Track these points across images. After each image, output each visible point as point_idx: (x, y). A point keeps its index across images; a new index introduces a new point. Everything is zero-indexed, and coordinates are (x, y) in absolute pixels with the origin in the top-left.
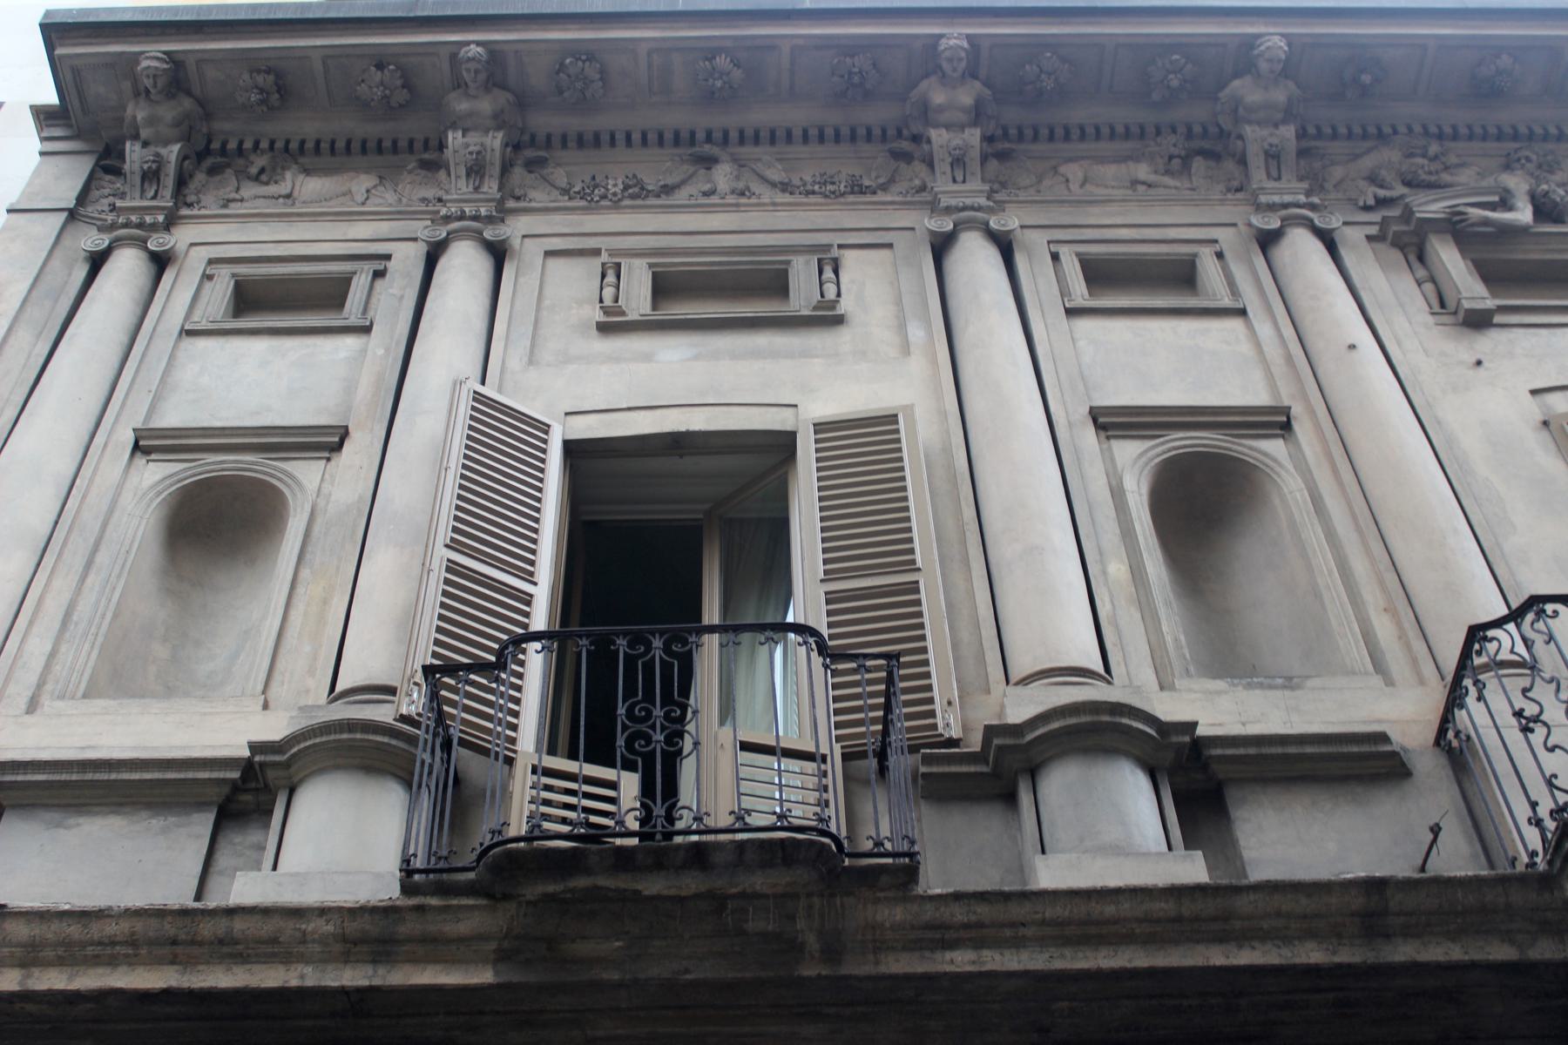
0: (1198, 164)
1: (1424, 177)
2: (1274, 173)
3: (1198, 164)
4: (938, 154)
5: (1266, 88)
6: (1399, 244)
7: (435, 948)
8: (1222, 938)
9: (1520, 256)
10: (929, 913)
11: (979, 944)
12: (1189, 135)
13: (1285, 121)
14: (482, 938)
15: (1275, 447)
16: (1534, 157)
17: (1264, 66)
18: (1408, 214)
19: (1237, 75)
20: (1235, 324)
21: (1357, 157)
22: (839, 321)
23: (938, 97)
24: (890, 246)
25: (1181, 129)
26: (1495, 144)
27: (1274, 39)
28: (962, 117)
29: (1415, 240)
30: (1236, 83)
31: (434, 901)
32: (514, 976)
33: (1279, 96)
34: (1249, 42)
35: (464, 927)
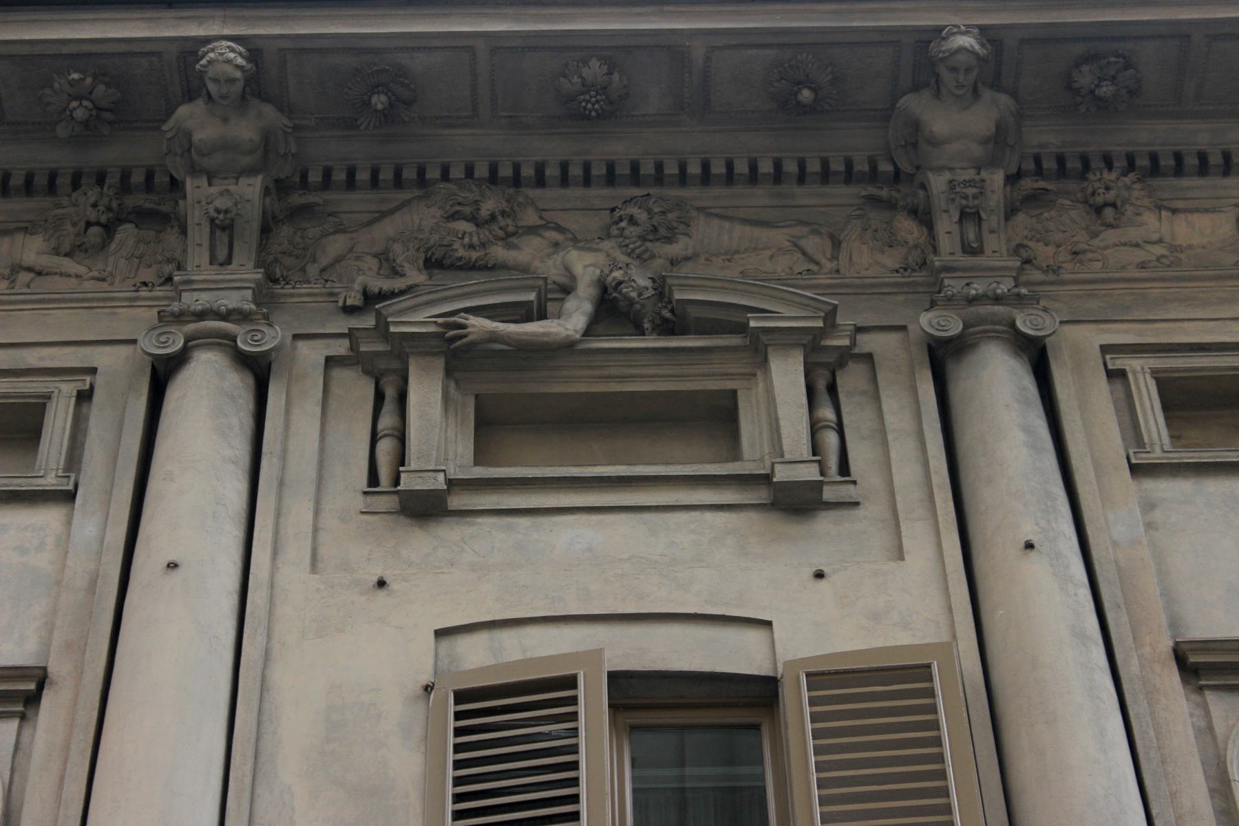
1: (461, 252)
2: (222, 254)
3: (126, 233)
5: (225, 120)
9: (557, 389)
12: (125, 186)
13: (251, 171)
16: (642, 216)
25: (113, 179)
26: (605, 192)
29: (396, 365)
30: (183, 111)
34: (191, 49)
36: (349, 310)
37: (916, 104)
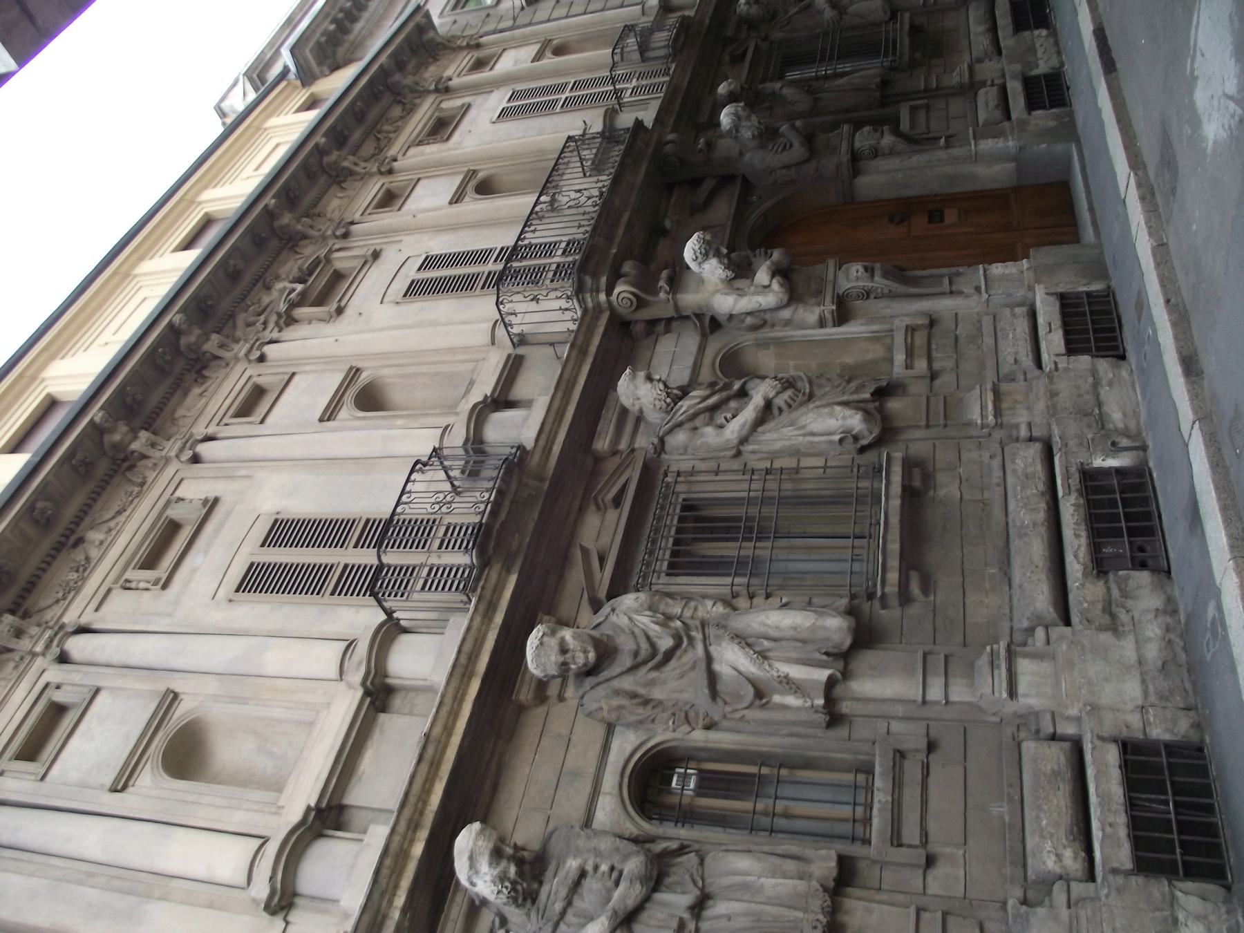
0: (206, 373)
4: (144, 451)
6: (288, 324)
7: (498, 590)
8: (573, 386)
10: (539, 450)
11: (553, 443)
14: (500, 574)
15: (364, 375)
17: (184, 327)
18: (279, 315)
19: (178, 340)
20: (296, 378)
21: (234, 327)
22: (216, 501)
23: (117, 437)
24: (182, 480)
27: (174, 316)
28: (131, 435)
31: (482, 583)
32: (517, 567)
33: (197, 331)
34: (171, 325)
35: (494, 575)
36: (264, 329)
37: (276, 224)
